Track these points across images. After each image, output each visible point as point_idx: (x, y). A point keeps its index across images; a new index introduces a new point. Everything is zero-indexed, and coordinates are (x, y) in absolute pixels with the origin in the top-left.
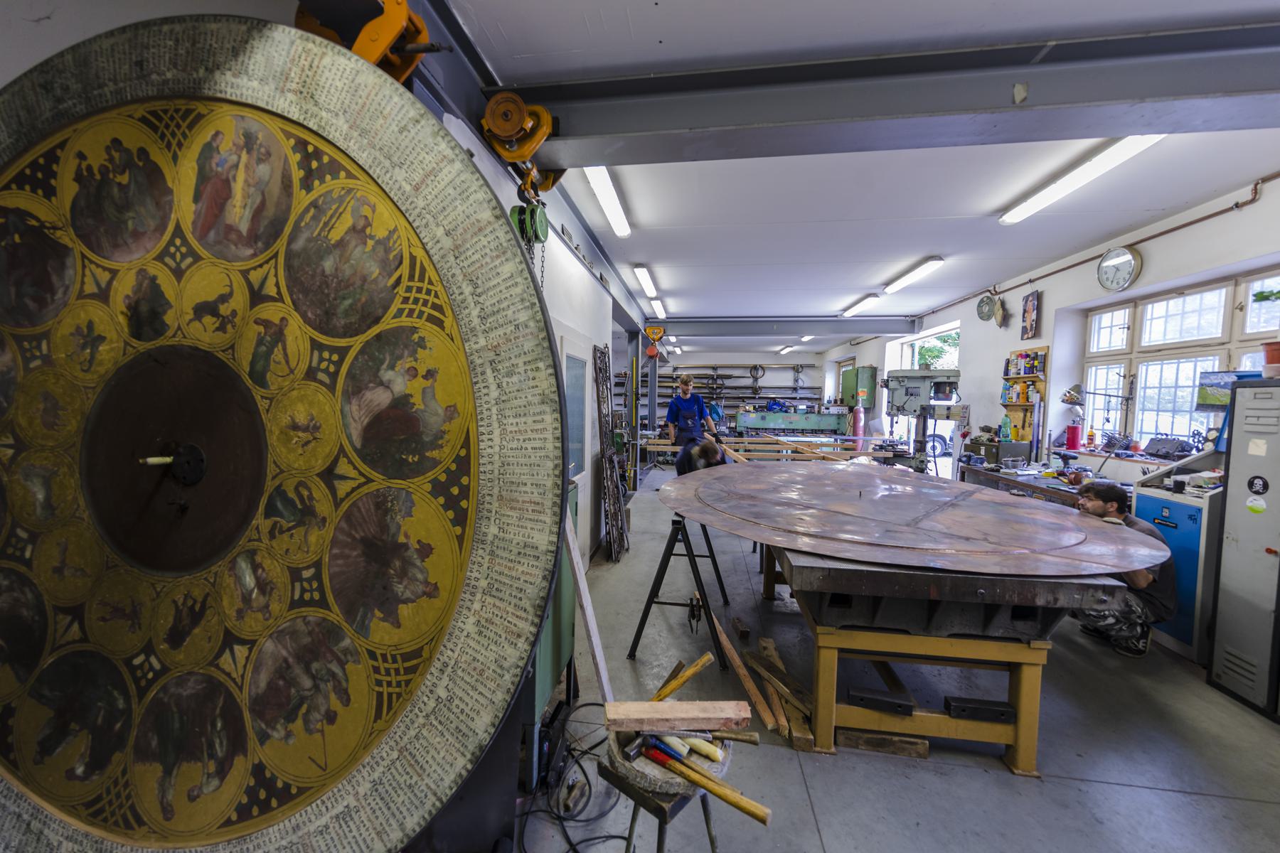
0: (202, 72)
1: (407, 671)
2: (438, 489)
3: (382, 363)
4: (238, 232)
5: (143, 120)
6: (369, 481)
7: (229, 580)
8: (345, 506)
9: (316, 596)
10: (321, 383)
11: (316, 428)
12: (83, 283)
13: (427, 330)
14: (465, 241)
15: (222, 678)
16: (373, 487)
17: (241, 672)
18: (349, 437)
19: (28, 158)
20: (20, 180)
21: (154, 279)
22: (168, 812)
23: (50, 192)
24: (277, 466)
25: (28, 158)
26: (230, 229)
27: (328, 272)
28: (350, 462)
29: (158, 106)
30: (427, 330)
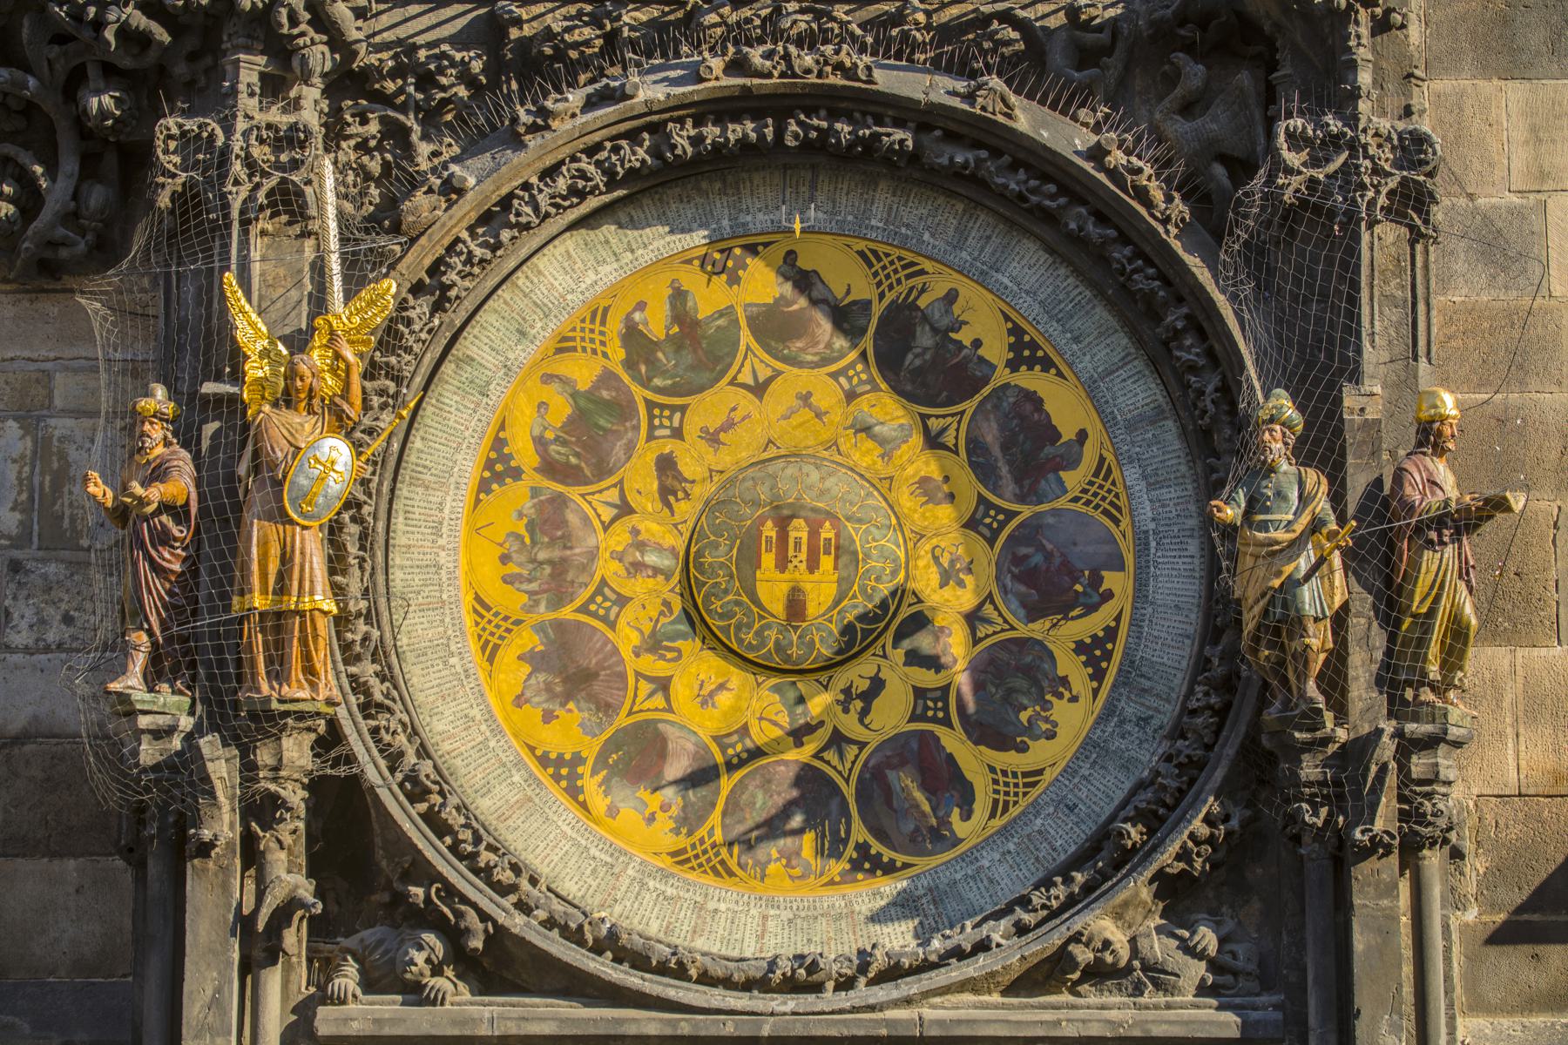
0: (1011, 847)
1: (487, 642)
2: (578, 760)
5: (1040, 772)
6: (630, 713)
9: (593, 607)
10: (729, 735)
11: (704, 703)
12: (996, 608)
13: (682, 841)
14: (699, 917)
15: (603, 484)
17: (595, 503)
18: (672, 723)
19: (1117, 657)
20: (1111, 633)
21: (937, 672)
23: (1080, 648)
25: (1117, 657)
26: (903, 763)
28: (657, 709)
30: (682, 841)
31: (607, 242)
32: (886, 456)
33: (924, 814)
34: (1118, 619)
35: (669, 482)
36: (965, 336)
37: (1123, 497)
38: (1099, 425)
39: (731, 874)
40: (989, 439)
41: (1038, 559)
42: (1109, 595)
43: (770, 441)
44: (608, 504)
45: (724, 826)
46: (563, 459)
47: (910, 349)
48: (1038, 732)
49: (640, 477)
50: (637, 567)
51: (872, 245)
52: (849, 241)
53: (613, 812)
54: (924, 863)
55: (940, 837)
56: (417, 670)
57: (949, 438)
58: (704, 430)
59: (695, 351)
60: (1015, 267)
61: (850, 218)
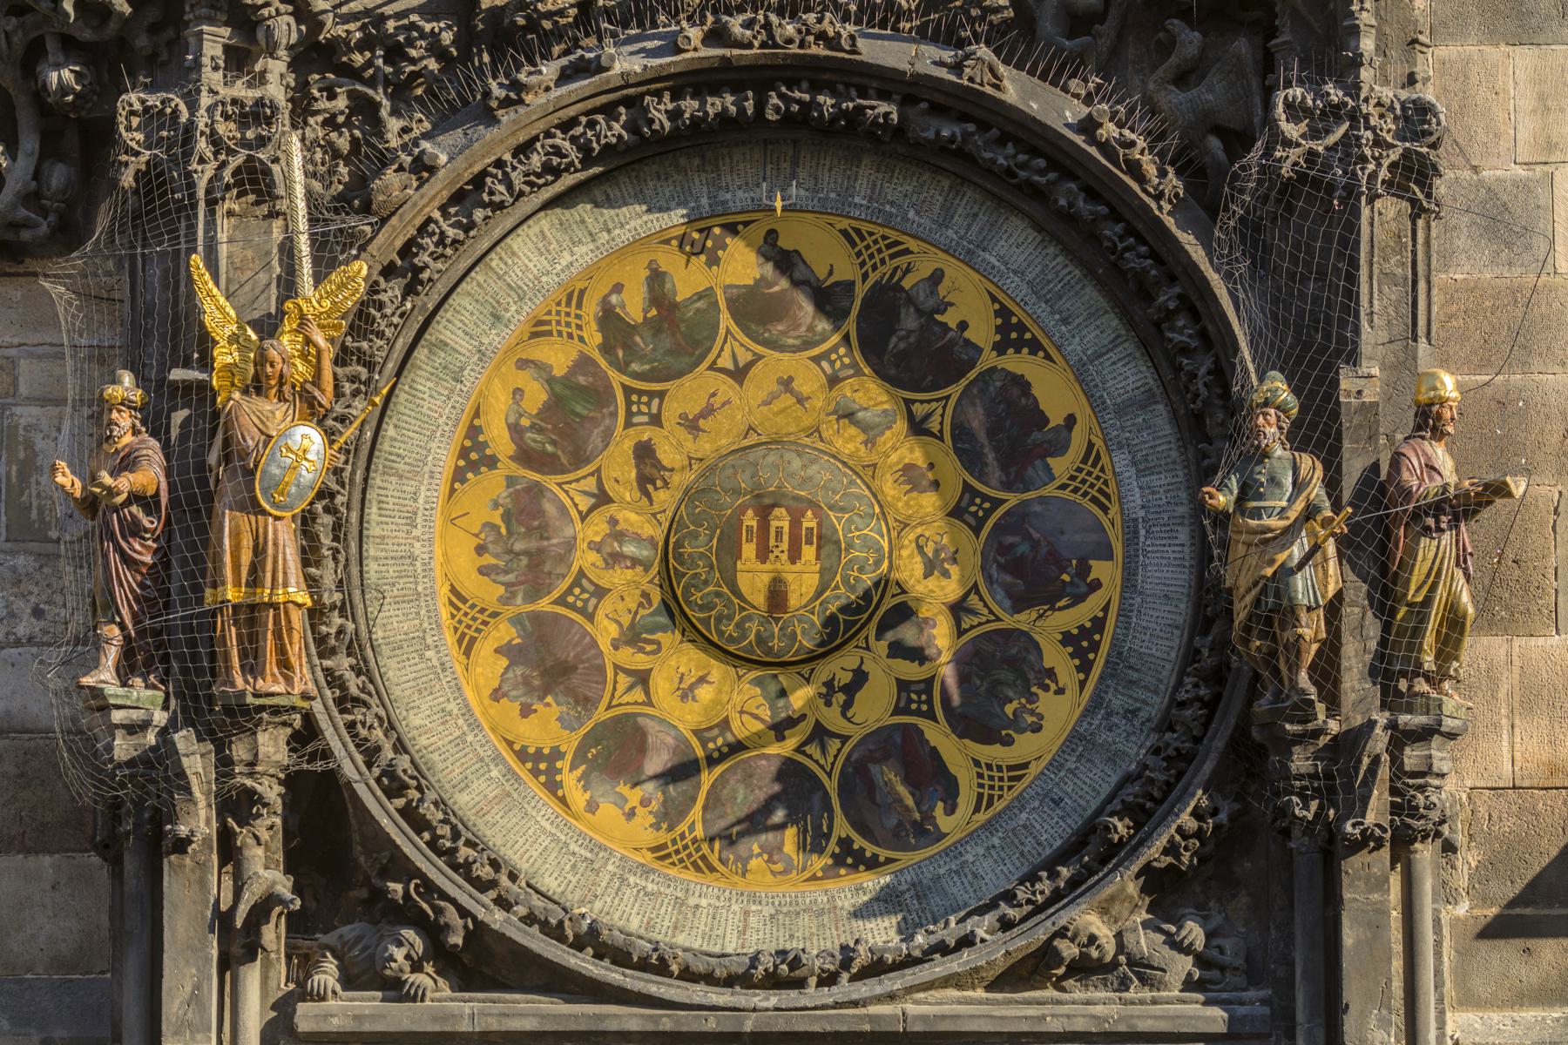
0: (996, 841)
1: (464, 635)
2: (557, 754)
5: (1026, 766)
6: (609, 707)
7: (648, 530)
9: (571, 599)
10: (710, 729)
11: (684, 697)
12: (981, 599)
13: (663, 837)
14: (680, 912)
16: (603, 705)
17: (572, 493)
18: (652, 717)
19: (1105, 648)
20: (1099, 624)
21: (921, 664)
23: (1067, 639)
25: (1105, 648)
26: (885, 758)
28: (636, 703)
29: (1020, 786)
30: (663, 837)
31: (583, 221)
32: (870, 443)
33: (907, 809)
34: (1106, 609)
35: (648, 470)
36: (950, 318)
37: (1112, 484)
38: (1088, 410)
39: (712, 869)
40: (975, 424)
41: (1024, 548)
42: (1096, 585)
43: (750, 428)
44: (585, 493)
45: (704, 821)
46: (538, 447)
47: (894, 332)
48: (1023, 725)
50: (614, 559)
51: (855, 224)
52: (832, 219)
53: (592, 807)
54: (908, 858)
55: (924, 832)
56: (392, 663)
57: (934, 424)
59: (673, 335)
60: (1002, 246)
61: (833, 195)
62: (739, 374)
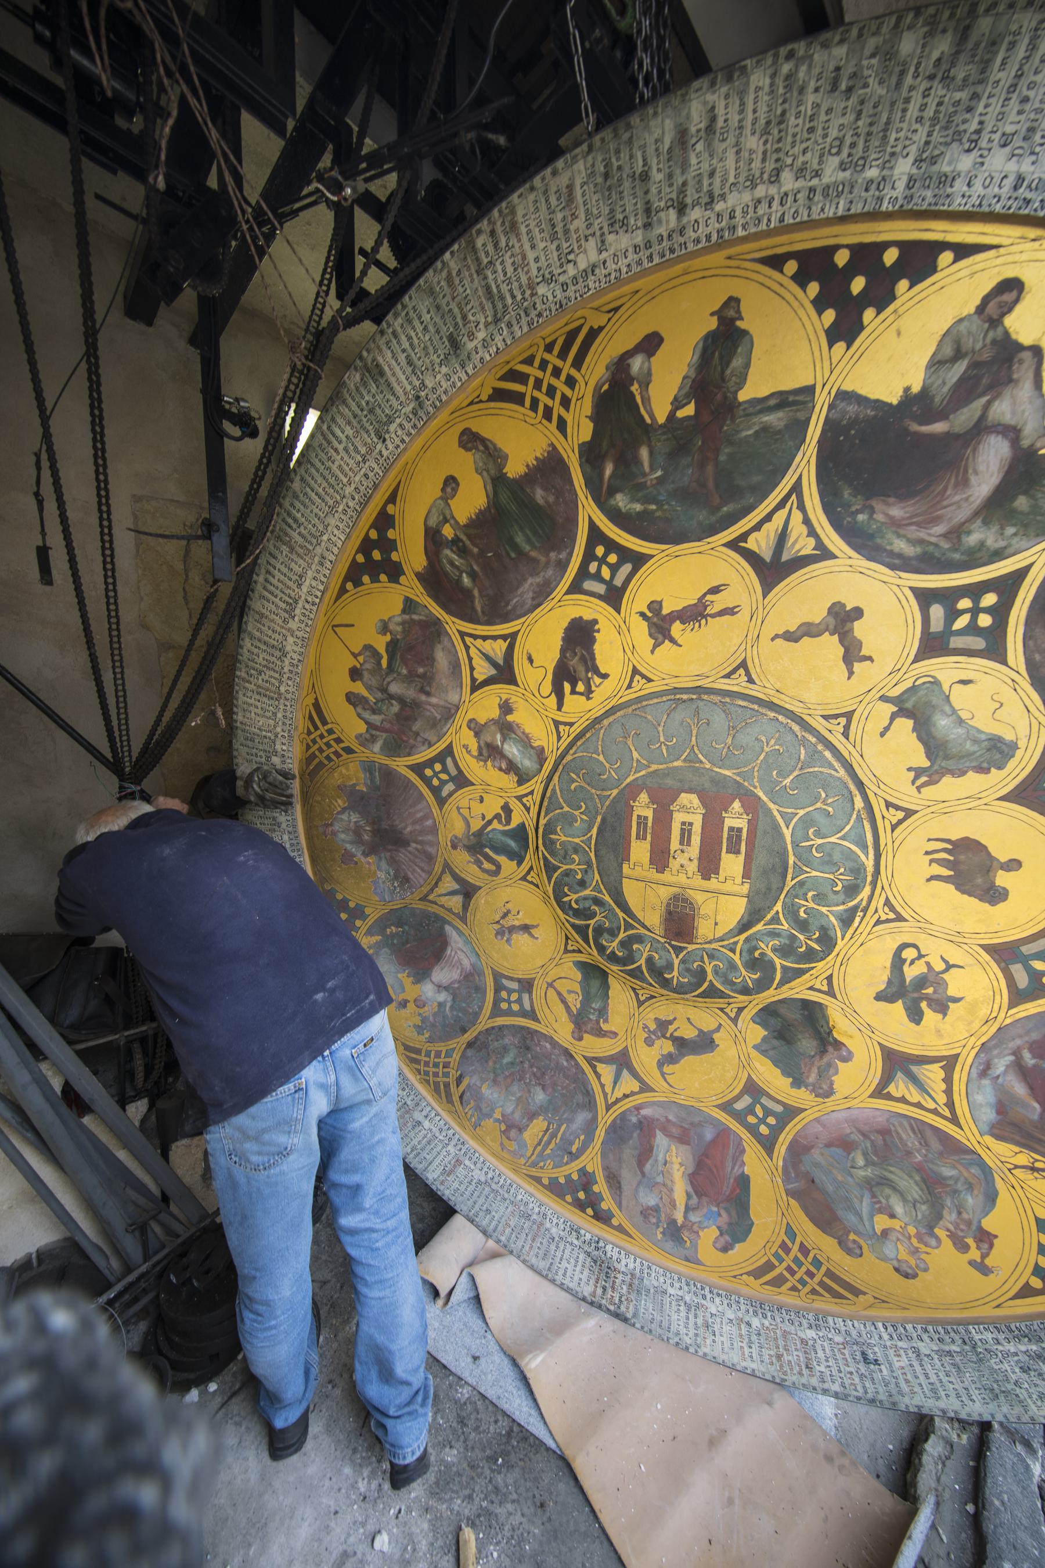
1: (313, 756)
3: (452, 1007)
4: (667, 1134)
8: (438, 868)
9: (428, 772)
10: (511, 979)
11: (500, 933)
12: (948, 1080)
17: (473, 651)
22: (470, 440)
24: (532, 883)
26: (683, 1139)
27: (538, 1089)
30: (419, 1041)
32: (925, 776)
33: (673, 1204)
35: (574, 662)
43: (743, 665)
44: (487, 658)
45: (463, 1056)
49: (541, 636)
50: (490, 752)
58: (655, 606)
62: (772, 571)
